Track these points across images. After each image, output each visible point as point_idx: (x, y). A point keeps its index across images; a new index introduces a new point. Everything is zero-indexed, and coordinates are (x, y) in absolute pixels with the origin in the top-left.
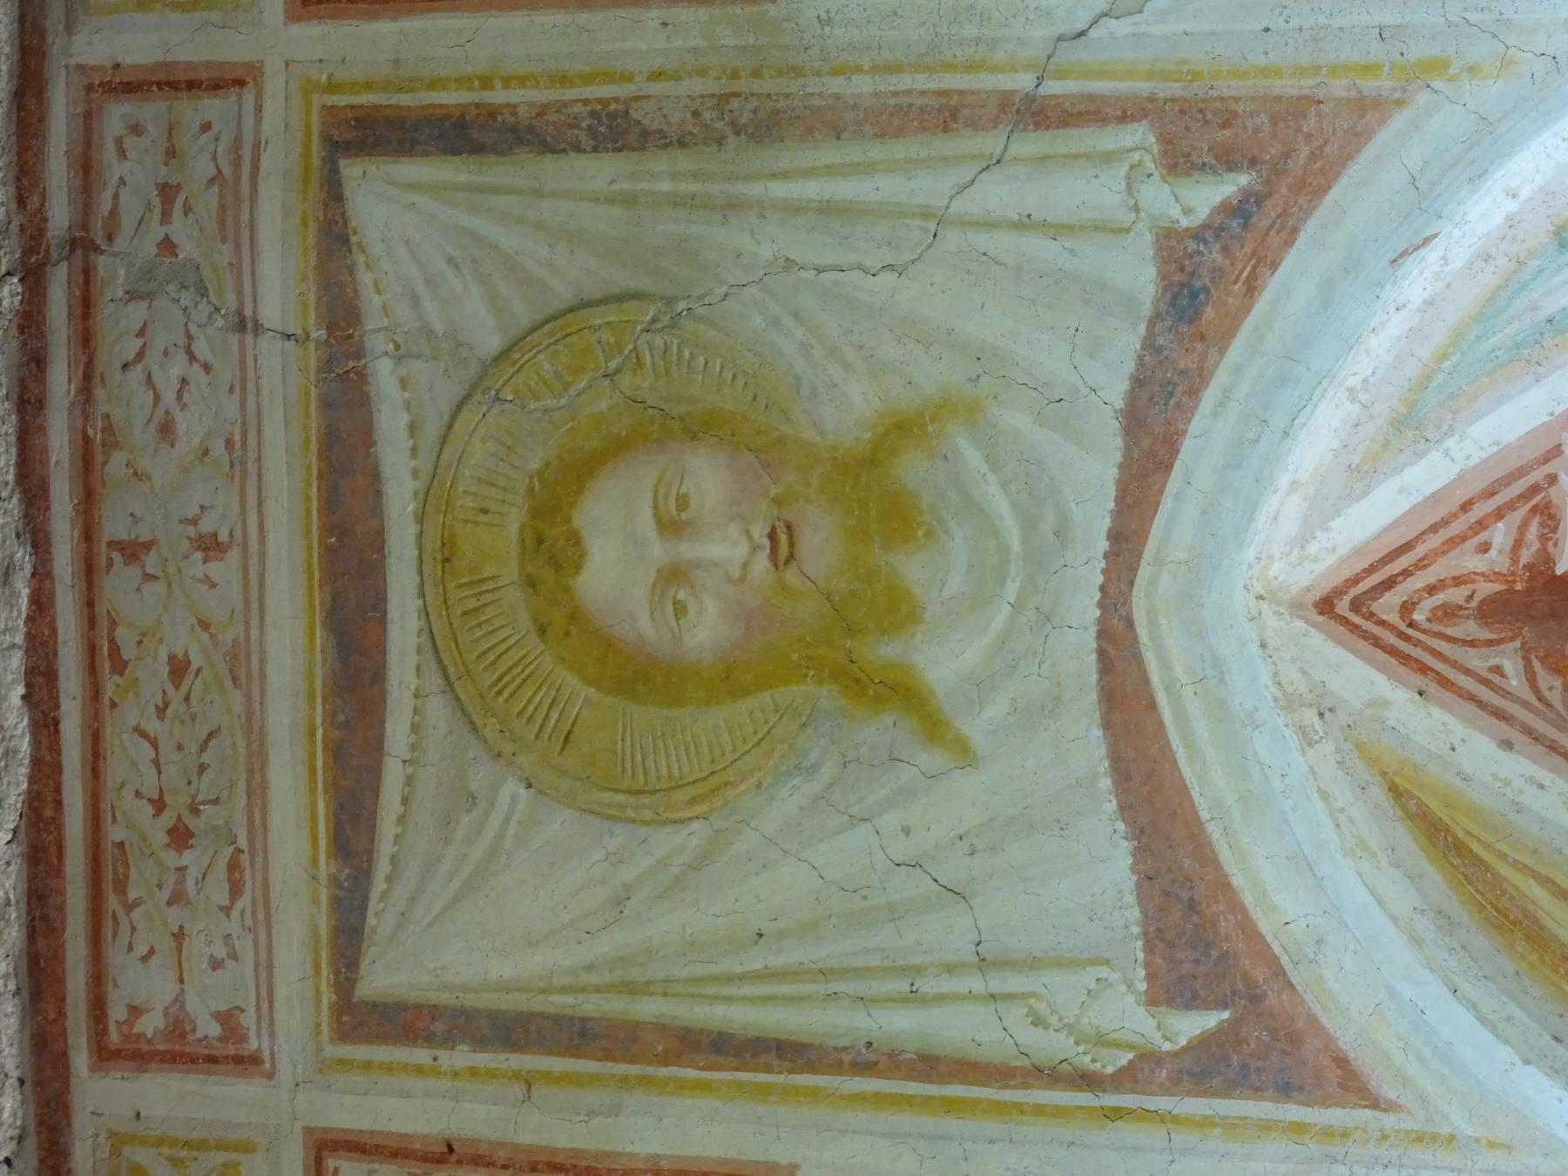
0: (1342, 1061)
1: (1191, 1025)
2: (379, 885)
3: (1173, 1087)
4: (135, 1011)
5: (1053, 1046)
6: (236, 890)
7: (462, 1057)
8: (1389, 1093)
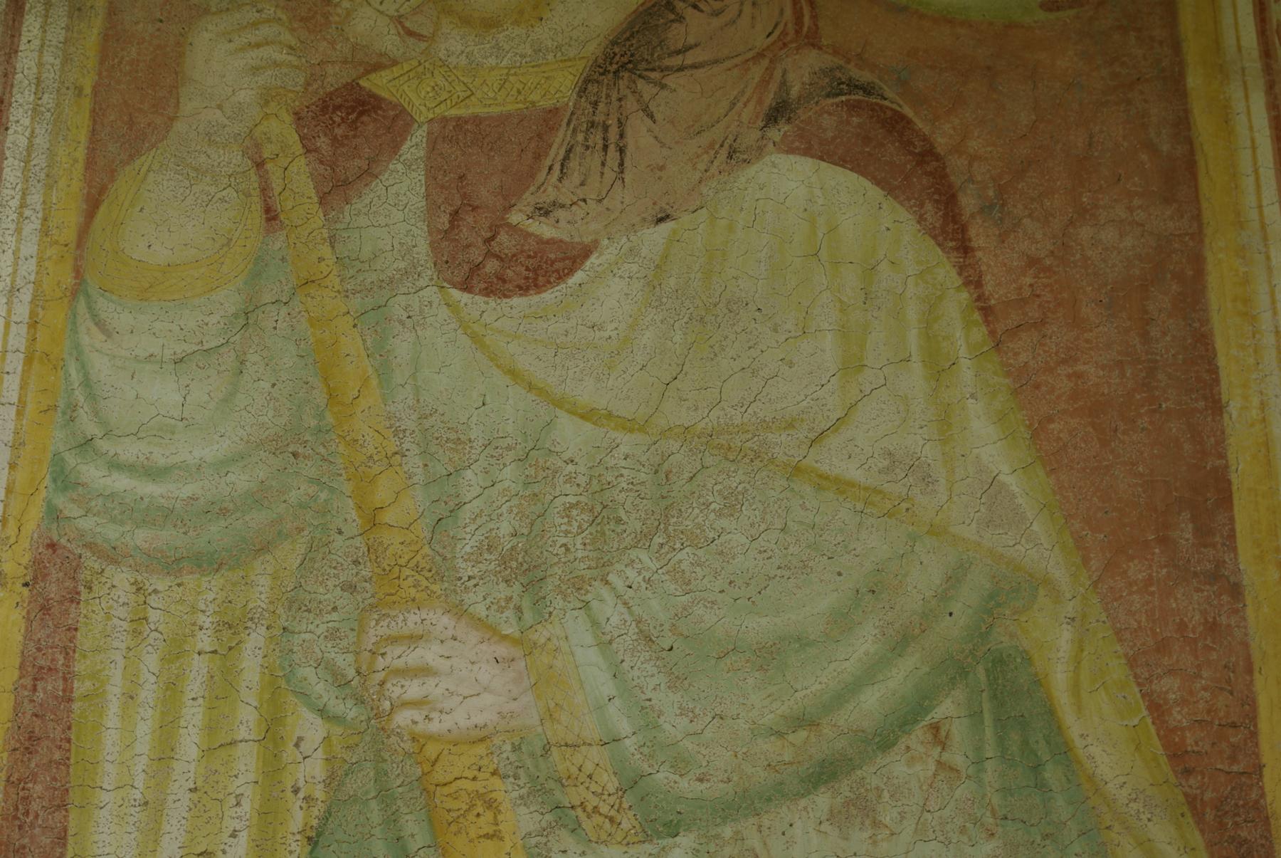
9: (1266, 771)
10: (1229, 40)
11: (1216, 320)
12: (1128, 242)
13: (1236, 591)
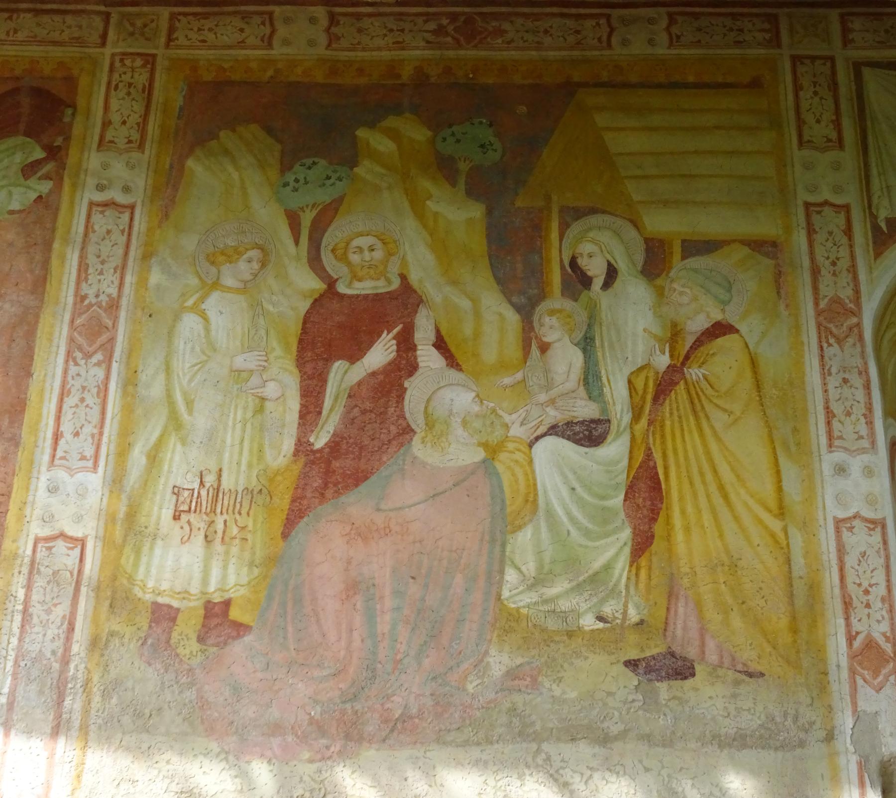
0: (881, 253)
1: (883, 225)
2: (883, 71)
3: (871, 222)
4: (852, 22)
5: (875, 200)
6: (879, 42)
7: (854, 88)
8: (878, 261)
9: (9, 512)
10: (74, 229)
11: (38, 342)
12: (13, 309)
13: (17, 445)
